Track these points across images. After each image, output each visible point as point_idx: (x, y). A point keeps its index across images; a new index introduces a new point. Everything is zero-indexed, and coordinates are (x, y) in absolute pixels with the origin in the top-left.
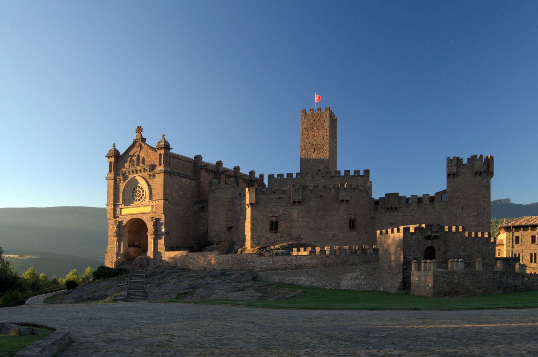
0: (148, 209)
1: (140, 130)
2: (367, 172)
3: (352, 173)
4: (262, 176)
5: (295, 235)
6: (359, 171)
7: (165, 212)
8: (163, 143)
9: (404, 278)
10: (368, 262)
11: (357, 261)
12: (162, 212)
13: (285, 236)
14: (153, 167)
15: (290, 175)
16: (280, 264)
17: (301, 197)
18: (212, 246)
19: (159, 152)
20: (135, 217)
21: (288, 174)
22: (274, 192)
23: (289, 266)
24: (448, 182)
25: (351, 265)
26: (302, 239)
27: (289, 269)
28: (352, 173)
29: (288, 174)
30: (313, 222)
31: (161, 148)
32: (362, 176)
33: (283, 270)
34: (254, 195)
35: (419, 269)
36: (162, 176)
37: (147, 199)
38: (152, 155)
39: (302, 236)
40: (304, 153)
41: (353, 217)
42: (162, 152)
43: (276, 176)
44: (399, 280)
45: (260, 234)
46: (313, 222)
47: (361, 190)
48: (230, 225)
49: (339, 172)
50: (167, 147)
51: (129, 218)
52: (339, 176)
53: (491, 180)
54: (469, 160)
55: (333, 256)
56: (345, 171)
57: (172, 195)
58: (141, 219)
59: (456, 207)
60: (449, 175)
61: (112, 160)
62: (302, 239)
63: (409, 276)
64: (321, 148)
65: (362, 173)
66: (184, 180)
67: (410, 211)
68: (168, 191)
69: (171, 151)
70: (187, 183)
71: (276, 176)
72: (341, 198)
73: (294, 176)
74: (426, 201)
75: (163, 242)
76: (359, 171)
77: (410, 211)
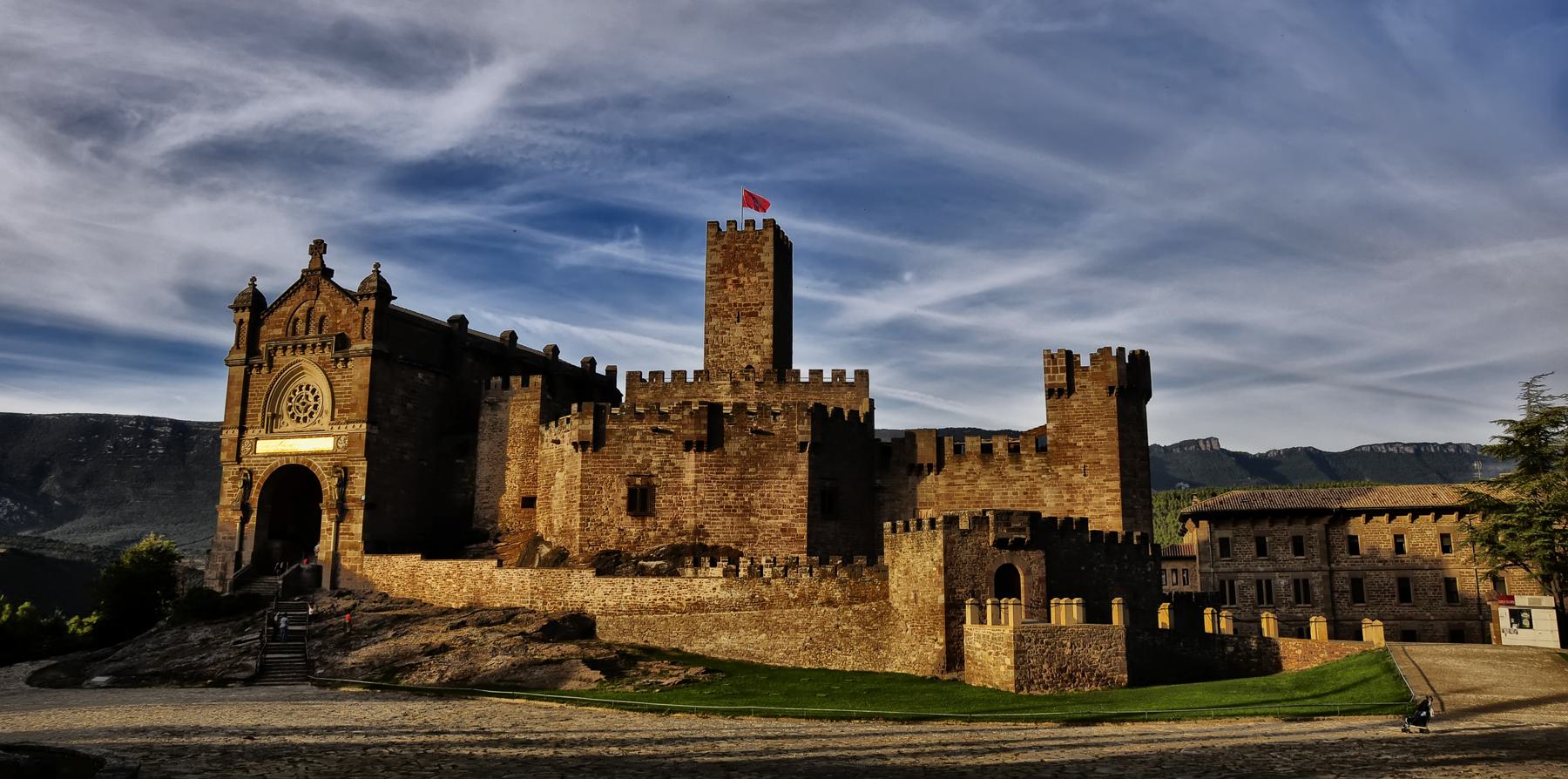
0: (326, 444)
2: (863, 375)
3: (827, 377)
4: (612, 372)
5: (691, 522)
6: (844, 372)
7: (368, 455)
8: (375, 284)
9: (948, 642)
10: (863, 600)
11: (838, 595)
12: (361, 453)
13: (665, 527)
14: (342, 343)
15: (679, 375)
16: (651, 597)
17: (704, 432)
18: (484, 545)
19: (362, 304)
20: (292, 461)
21: (674, 373)
22: (639, 417)
23: (673, 605)
24: (1049, 408)
25: (822, 604)
26: (708, 535)
27: (674, 610)
28: (827, 377)
29: (674, 373)
31: (369, 296)
32: (851, 385)
33: (657, 612)
35: (982, 620)
36: (366, 365)
37: (326, 419)
38: (344, 311)
39: (707, 527)
40: (713, 323)
41: (828, 484)
42: (371, 304)
43: (646, 376)
44: (936, 646)
45: (604, 520)
48: (530, 492)
49: (798, 372)
50: (383, 291)
51: (277, 463)
52: (797, 381)
55: (779, 581)
56: (812, 372)
58: (307, 469)
59: (1070, 467)
60: (1050, 393)
61: (246, 315)
62: (708, 535)
63: (961, 636)
65: (850, 377)
67: (963, 473)
68: (380, 401)
71: (646, 376)
72: (801, 438)
73: (690, 378)
75: (360, 531)
76: (844, 372)
77: (963, 473)
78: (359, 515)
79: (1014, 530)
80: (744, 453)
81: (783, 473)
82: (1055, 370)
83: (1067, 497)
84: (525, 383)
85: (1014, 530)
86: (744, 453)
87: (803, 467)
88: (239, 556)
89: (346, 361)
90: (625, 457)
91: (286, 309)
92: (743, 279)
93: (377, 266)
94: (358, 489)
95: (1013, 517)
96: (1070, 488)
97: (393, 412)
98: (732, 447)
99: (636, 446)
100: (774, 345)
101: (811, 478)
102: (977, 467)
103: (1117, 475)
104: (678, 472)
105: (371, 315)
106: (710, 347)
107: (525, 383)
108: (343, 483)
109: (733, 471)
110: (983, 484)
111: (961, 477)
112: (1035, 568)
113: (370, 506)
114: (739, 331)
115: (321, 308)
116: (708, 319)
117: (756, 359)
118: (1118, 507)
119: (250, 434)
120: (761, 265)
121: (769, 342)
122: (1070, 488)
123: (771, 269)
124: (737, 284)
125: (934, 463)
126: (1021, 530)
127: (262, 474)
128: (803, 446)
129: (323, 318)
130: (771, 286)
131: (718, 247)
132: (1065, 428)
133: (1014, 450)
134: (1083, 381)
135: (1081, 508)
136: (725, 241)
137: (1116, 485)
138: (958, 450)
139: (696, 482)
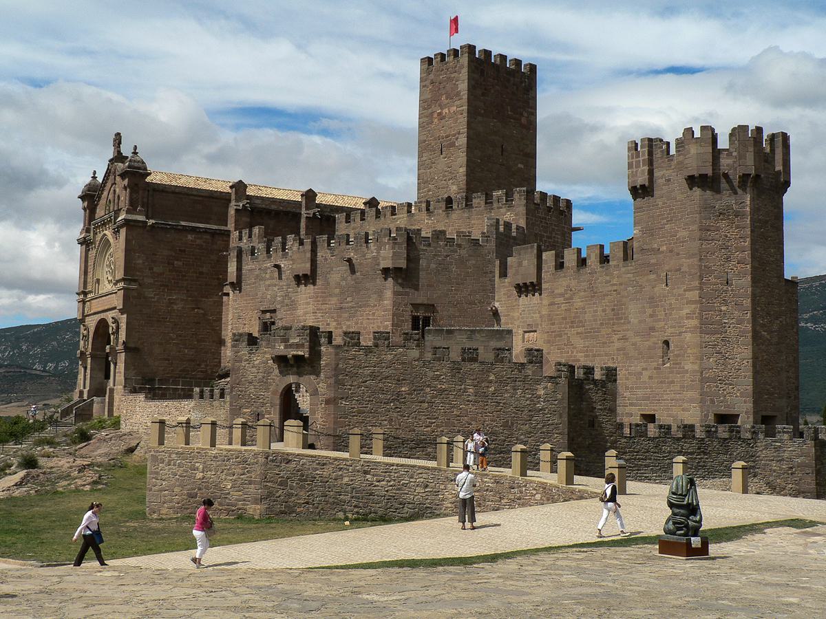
1: (118, 139)
14: (117, 212)
17: (308, 265)
30: (334, 324)
34: (235, 263)
40: (424, 159)
46: (334, 324)
47: (394, 239)
51: (98, 317)
53: (785, 197)
54: (680, 143)
57: (151, 269)
59: (652, 277)
64: (453, 145)
66: (190, 237)
67: (561, 290)
69: (148, 179)
70: (198, 241)
74: (593, 261)
78: (122, 357)
79: (291, 346)
80: (344, 283)
81: (372, 301)
82: (638, 166)
83: (649, 311)
84: (250, 236)
85: (291, 346)
86: (344, 283)
87: (389, 294)
88: (81, 393)
89: (118, 231)
90: (260, 294)
91: (105, 193)
92: (446, 110)
93: (135, 148)
94: (123, 336)
95: (293, 333)
96: (652, 300)
97: (155, 269)
98: (335, 277)
99: (268, 282)
100: (468, 175)
101: (395, 304)
102: (573, 283)
103: (696, 283)
104: (292, 306)
105: (128, 190)
106: (422, 182)
107: (250, 236)
108: (117, 332)
109: (334, 300)
110: (578, 302)
111: (562, 295)
112: (322, 387)
113: (127, 348)
114: (442, 161)
115: (117, 190)
116: (420, 156)
117: (455, 188)
118: (694, 322)
119: (89, 296)
120: (458, 94)
121: (463, 170)
122: (652, 300)
123: (466, 97)
124: (441, 117)
125: (535, 281)
126: (298, 346)
127: (92, 330)
128: (386, 271)
129: (119, 196)
130: (466, 115)
131: (427, 83)
132: (649, 231)
133: (604, 259)
134: (667, 173)
135: (662, 324)
136: (432, 76)
137: (695, 295)
138: (560, 266)
139: (305, 313)
